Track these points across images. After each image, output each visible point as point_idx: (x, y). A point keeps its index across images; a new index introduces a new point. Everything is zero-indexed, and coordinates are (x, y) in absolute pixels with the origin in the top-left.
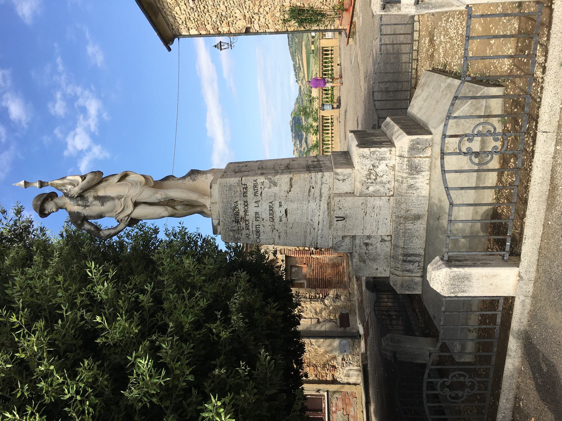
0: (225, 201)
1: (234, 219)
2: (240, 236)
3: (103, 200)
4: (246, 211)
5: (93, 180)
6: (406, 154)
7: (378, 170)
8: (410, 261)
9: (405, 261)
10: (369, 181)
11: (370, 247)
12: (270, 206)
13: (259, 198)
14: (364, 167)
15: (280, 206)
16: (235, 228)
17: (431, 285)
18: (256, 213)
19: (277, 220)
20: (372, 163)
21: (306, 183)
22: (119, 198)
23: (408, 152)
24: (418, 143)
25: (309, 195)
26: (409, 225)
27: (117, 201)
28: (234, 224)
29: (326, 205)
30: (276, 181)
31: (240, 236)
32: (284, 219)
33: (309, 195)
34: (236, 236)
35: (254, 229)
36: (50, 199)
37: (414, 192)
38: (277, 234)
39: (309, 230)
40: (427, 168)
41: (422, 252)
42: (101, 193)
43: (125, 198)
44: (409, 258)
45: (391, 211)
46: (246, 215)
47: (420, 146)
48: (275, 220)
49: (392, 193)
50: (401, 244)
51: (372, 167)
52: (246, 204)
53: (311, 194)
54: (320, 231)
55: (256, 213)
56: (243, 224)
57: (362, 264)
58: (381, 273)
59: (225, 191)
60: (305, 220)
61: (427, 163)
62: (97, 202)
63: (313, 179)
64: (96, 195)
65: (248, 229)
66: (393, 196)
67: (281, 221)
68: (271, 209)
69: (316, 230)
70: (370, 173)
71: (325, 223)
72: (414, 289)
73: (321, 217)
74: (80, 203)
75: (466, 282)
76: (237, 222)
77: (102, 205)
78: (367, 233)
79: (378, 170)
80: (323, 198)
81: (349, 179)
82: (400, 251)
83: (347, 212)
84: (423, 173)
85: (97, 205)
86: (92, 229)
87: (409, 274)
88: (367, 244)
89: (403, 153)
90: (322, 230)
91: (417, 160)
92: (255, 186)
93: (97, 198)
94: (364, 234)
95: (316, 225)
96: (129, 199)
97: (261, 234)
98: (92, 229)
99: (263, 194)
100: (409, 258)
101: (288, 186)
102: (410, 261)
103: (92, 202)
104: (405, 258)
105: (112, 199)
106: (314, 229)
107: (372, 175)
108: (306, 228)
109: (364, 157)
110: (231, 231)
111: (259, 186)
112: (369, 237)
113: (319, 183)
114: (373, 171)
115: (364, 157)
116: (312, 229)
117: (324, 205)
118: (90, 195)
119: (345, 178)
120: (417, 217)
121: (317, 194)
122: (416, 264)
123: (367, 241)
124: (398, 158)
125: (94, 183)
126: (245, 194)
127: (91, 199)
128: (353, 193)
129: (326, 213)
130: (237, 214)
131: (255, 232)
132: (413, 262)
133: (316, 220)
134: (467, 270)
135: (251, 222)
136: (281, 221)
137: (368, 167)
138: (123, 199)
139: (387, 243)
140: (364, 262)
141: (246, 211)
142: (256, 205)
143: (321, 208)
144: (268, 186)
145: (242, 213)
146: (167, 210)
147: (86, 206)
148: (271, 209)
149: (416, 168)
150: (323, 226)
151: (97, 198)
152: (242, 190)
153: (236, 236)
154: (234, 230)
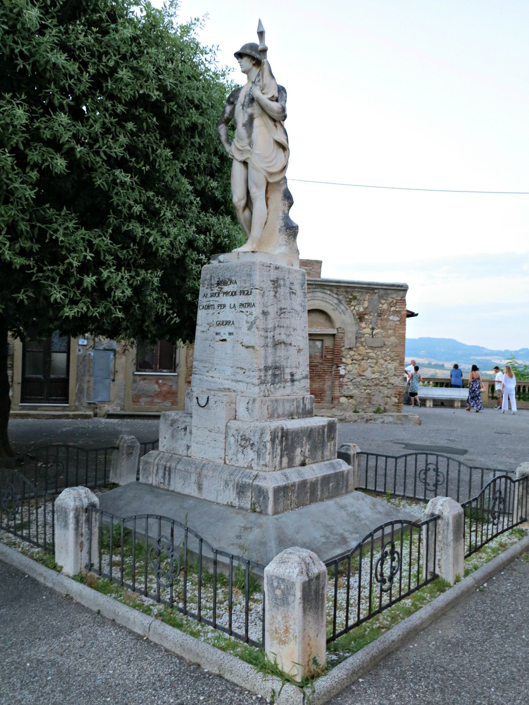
0: (238, 269)
1: (221, 280)
2: (206, 286)
3: (250, 123)
4: (226, 293)
5: (272, 110)
6: (256, 483)
7: (249, 448)
8: (165, 474)
9: (165, 467)
10: (240, 439)
11: (183, 432)
12: (230, 322)
13: (238, 309)
14: (252, 434)
15: (230, 334)
16: (213, 281)
17: (67, 489)
18: (225, 306)
19: (218, 329)
20: (256, 444)
21: (248, 365)
22: (250, 144)
23: (257, 485)
24: (264, 498)
25: (238, 367)
26: (194, 478)
27: (247, 141)
28: (217, 280)
29: (227, 386)
30: (252, 330)
31: (206, 286)
32: (218, 338)
33: (238, 367)
34: (206, 282)
35: (211, 303)
36: (254, 62)
37: (222, 487)
38: (205, 329)
39: (207, 365)
40: (242, 505)
41: (171, 488)
42: (257, 122)
43: (250, 151)
44: (167, 473)
45: (211, 459)
46: (224, 293)
47: (261, 499)
48: (218, 328)
49: (227, 462)
50: (179, 467)
51: (251, 442)
52: (234, 294)
53: (239, 370)
54: (205, 378)
55: (225, 306)
56: (216, 290)
57: (170, 422)
58: (162, 442)
59: (246, 269)
60: (216, 361)
61: (246, 505)
62: (246, 118)
63: (252, 374)
64: (255, 116)
65: (212, 296)
66: (225, 463)
67: (217, 334)
68: (228, 323)
69: (207, 374)
70: (247, 440)
71: (212, 384)
72: (143, 475)
73: (217, 380)
74: (247, 98)
75: (63, 524)
76: (218, 284)
77: (244, 125)
78: (194, 431)
79: (249, 448)
80: (234, 384)
81: (248, 415)
82: (173, 465)
83: (212, 411)
84: (237, 499)
85: (244, 118)
86: (226, 115)
87: (155, 471)
88: (185, 429)
89: (258, 479)
90: (207, 381)
91: (249, 494)
92: (249, 305)
93: (251, 118)
94: (193, 427)
95: (211, 374)
96: (249, 156)
97: (206, 311)
98: (226, 115)
99: (241, 313)
100: (167, 473)
101: (247, 344)
102: (165, 474)
103: (246, 112)
104: (167, 469)
105: (250, 136)
106: (208, 372)
107: (244, 442)
108: (209, 363)
109: (262, 434)
110: (211, 276)
111: (248, 309)
112: (191, 433)
113: (248, 380)
114: (248, 443)
115: (262, 434)
116: (208, 369)
117: (228, 384)
118: (255, 110)
119: (250, 411)
120: (200, 488)
121: (240, 377)
122: (162, 481)
123: (188, 430)
124: (256, 473)
125: (269, 112)
126: (242, 292)
127: (250, 110)
128: (235, 419)
129: (221, 387)
130: (225, 283)
131: (208, 303)
132: (164, 478)
133: (216, 374)
134: (72, 526)
135: (217, 299)
136: (217, 334)
137: (252, 438)
138: (249, 148)
139: (186, 451)
140: (171, 425)
141: (226, 293)
142: (232, 306)
143: (226, 381)
144: (249, 320)
145: (226, 289)
146: (240, 200)
147: (243, 105)
148: (228, 323)
149: (243, 492)
150: (210, 382)
151: (251, 118)
152: (246, 289)
153: (206, 282)
154: (211, 280)
